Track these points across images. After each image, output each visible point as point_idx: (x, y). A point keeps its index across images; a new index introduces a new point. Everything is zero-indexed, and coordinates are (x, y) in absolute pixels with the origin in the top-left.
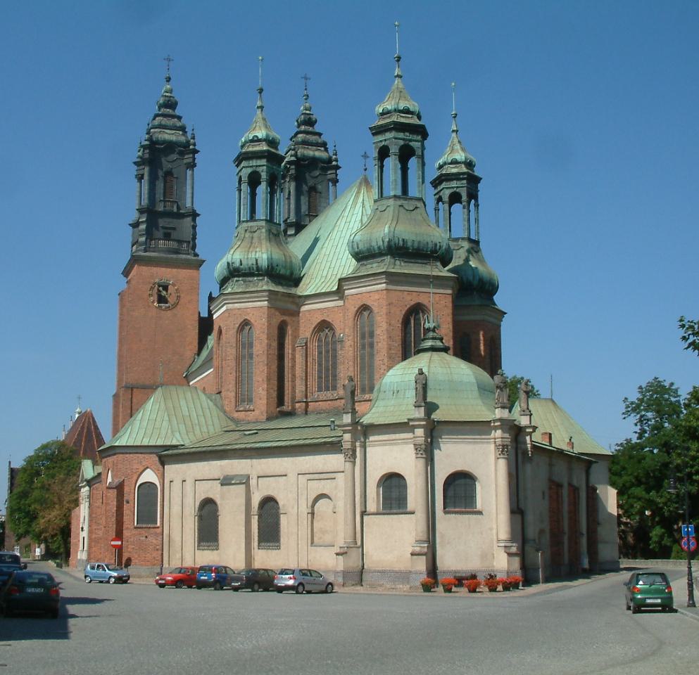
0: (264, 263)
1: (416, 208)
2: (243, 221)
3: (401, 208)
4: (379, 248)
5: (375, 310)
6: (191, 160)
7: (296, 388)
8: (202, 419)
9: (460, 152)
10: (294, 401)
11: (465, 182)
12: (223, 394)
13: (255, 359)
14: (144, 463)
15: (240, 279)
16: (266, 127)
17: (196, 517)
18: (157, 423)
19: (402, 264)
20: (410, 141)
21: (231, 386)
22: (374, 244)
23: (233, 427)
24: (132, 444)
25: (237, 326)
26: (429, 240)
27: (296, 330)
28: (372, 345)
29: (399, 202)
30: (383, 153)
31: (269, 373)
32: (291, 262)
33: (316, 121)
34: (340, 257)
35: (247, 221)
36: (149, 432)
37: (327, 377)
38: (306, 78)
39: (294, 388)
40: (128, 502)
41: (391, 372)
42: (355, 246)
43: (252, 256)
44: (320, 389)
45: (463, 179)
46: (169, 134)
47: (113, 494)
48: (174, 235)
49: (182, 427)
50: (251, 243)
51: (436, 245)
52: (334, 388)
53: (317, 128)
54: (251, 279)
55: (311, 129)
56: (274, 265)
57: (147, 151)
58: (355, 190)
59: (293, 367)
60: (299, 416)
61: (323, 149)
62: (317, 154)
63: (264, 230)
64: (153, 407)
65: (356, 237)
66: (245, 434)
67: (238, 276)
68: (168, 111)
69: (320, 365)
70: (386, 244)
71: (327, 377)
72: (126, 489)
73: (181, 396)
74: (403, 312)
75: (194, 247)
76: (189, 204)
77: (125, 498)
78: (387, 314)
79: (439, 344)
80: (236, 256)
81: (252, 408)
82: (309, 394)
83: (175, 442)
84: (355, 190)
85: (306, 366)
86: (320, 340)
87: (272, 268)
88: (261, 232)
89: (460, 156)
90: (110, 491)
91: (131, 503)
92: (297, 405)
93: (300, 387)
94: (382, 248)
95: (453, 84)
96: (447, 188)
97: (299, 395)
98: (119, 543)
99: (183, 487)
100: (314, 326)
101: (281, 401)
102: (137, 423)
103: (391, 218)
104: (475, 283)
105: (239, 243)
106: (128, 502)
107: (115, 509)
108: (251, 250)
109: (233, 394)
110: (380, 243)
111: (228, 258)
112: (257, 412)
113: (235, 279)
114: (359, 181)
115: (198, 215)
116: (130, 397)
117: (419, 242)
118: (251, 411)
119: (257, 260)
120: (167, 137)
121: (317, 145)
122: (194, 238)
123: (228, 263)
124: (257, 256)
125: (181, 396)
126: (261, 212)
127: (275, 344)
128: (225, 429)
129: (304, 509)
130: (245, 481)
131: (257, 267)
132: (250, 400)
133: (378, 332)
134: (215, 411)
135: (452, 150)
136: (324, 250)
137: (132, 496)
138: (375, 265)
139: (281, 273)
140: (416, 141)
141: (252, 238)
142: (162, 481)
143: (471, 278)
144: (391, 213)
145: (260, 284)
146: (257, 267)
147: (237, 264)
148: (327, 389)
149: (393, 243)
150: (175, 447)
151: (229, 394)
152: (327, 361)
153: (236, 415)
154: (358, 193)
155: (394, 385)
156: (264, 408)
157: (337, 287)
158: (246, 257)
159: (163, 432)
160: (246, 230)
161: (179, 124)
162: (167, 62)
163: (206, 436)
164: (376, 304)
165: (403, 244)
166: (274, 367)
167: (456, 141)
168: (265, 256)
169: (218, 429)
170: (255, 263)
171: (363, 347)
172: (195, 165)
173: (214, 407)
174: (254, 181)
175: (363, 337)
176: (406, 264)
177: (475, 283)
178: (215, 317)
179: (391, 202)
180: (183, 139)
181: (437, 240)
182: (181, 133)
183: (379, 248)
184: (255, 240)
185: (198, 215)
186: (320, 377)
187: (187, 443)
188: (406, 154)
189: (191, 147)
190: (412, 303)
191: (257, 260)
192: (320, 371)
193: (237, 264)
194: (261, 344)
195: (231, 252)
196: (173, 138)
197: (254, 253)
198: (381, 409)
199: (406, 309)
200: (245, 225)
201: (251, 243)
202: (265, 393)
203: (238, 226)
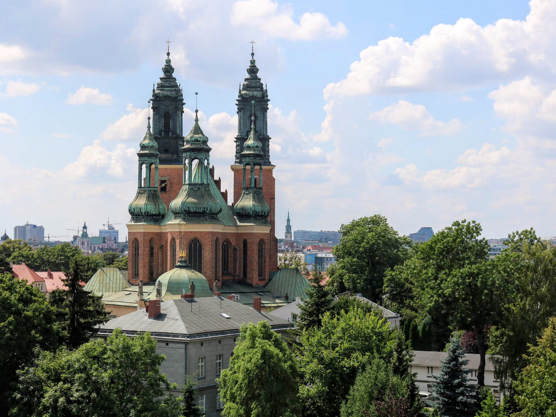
29: (191, 187)
38: (252, 43)
39: (158, 269)
56: (149, 211)
59: (158, 259)
62: (255, 93)
87: (148, 213)
121: (256, 87)
147: (133, 211)
149: (182, 209)
177: (251, 213)
181: (205, 206)
193: (133, 211)
196: (169, 93)
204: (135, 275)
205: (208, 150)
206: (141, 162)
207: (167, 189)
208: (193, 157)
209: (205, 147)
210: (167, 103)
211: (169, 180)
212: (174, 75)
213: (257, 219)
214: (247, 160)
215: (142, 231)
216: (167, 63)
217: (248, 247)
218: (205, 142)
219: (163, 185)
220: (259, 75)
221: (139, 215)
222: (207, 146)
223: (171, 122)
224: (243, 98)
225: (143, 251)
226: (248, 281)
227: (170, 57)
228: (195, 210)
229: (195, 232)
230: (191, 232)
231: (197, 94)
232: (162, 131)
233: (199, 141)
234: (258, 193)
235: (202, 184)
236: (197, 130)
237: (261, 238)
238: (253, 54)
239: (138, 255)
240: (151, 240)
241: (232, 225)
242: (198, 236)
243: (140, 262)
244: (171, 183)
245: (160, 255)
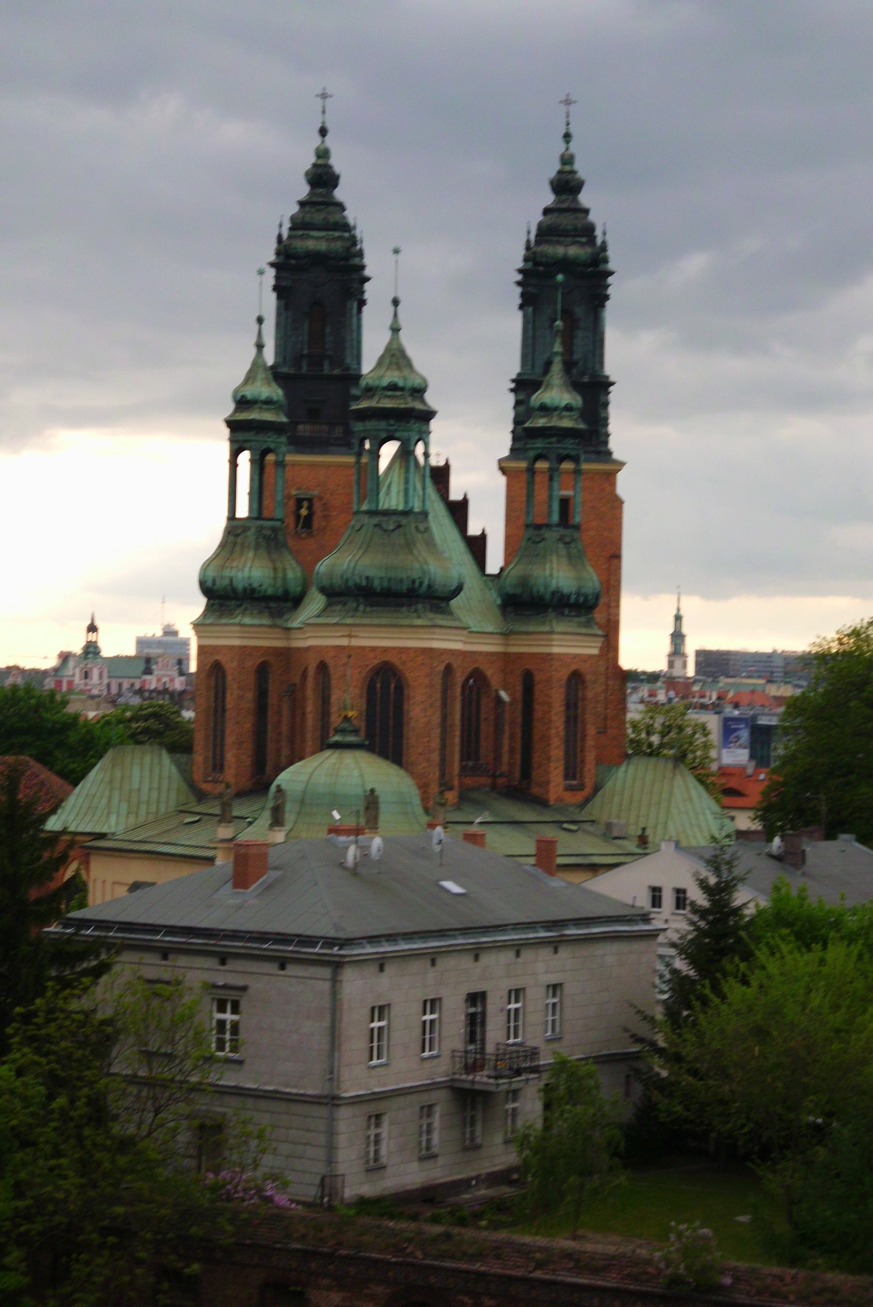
1: (399, 526)
8: (155, 794)
11: (553, 440)
13: (228, 714)
18: (96, 800)
19: (368, 609)
20: (396, 431)
26: (404, 576)
29: (376, 520)
32: (284, 578)
38: (568, 102)
39: (278, 750)
43: (227, 573)
45: (550, 436)
46: (318, 238)
51: (414, 581)
54: (228, 603)
56: (256, 585)
61: (584, 240)
62: (573, 251)
74: (364, 674)
83: (105, 830)
104: (548, 596)
117: (390, 579)
120: (311, 245)
128: (182, 808)
139: (270, 591)
140: (405, 431)
141: (235, 544)
143: (542, 590)
147: (209, 584)
150: (102, 836)
162: (319, 101)
165: (368, 583)
177: (548, 596)
181: (415, 575)
184: (238, 549)
190: (376, 662)
196: (322, 246)
204: (214, 768)
205: (428, 415)
206: (236, 446)
207: (316, 523)
208: (383, 435)
209: (418, 406)
210: (318, 275)
211: (320, 498)
212: (339, 194)
213: (562, 614)
214: (539, 443)
215: (237, 642)
216: (319, 156)
217: (537, 693)
218: (419, 392)
219: (304, 512)
220: (585, 198)
222: (423, 402)
223: (328, 330)
224: (537, 264)
225: (239, 697)
226: (536, 790)
227: (329, 141)
228: (385, 584)
229: (386, 650)
230: (373, 649)
231: (396, 251)
232: (302, 356)
233: (402, 389)
234: (568, 539)
235: (406, 513)
236: (395, 356)
237: (574, 667)
238: (567, 136)
239: (224, 710)
240: (262, 670)
241: (490, 629)
242: (395, 660)
243: (228, 731)
244: (326, 508)
245: (286, 712)
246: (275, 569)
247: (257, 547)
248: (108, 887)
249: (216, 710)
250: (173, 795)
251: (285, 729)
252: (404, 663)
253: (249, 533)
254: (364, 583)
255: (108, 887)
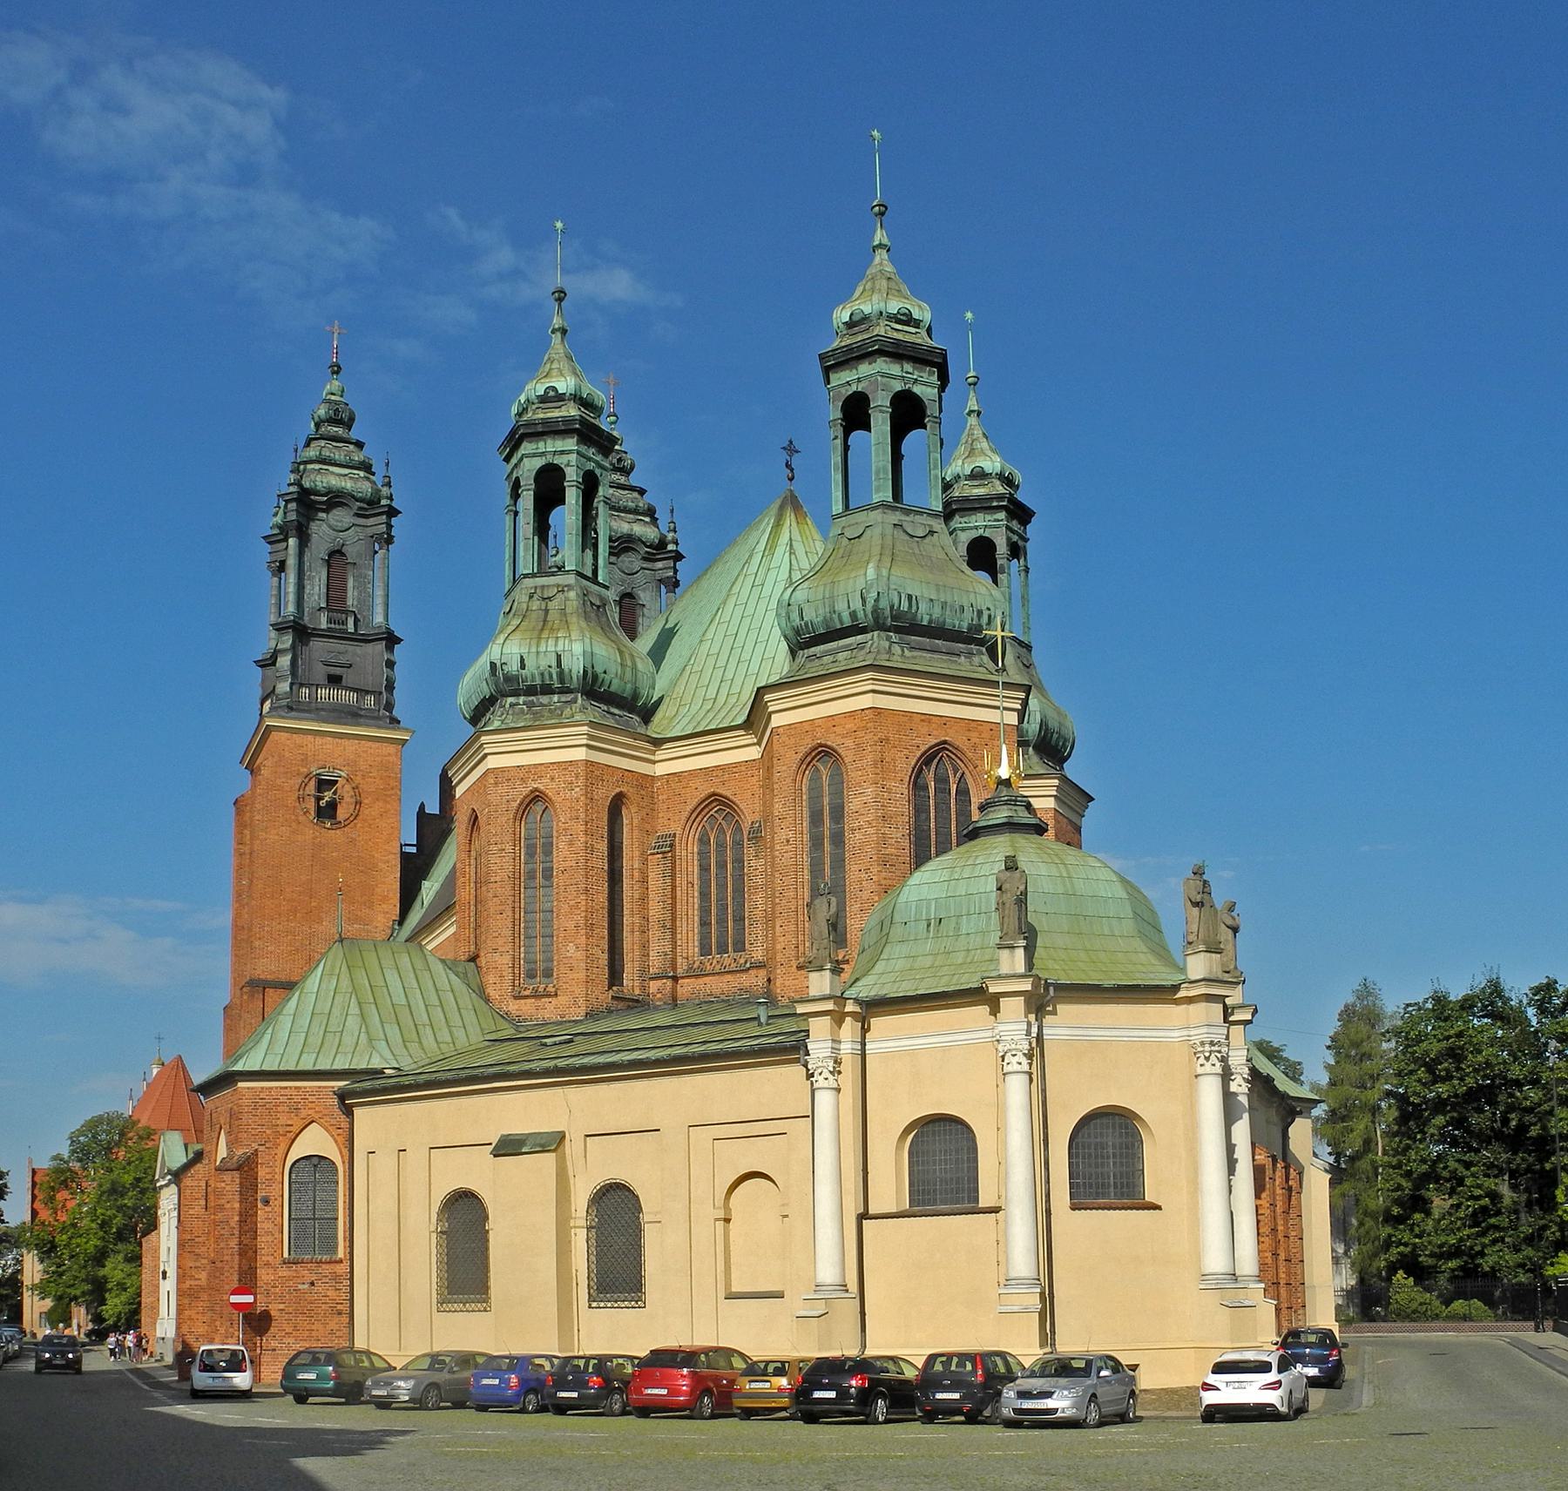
0: (575, 665)
1: (932, 533)
2: (526, 576)
3: (899, 533)
4: (853, 615)
5: (848, 757)
6: (383, 528)
7: (646, 950)
8: (438, 1014)
9: (989, 453)
10: (645, 976)
12: (482, 961)
14: (304, 1113)
15: (521, 699)
16: (575, 374)
17: (434, 1235)
21: (500, 941)
22: (841, 606)
23: (509, 1032)
24: (275, 1068)
25: (515, 805)
27: (650, 814)
28: (838, 839)
30: (856, 413)
31: (590, 912)
33: (632, 468)
34: (746, 656)
35: (533, 575)
36: (315, 1040)
37: (722, 921)
39: (645, 946)
40: (266, 1202)
41: (917, 877)
42: (795, 616)
44: (705, 950)
47: (230, 1184)
48: (349, 678)
49: (393, 1032)
50: (545, 621)
51: (980, 613)
52: (740, 946)
53: (634, 480)
54: (544, 699)
55: (623, 480)
56: (599, 670)
57: (293, 506)
58: (768, 522)
59: (644, 899)
60: (656, 1008)
63: (572, 594)
64: (324, 986)
65: (797, 593)
66: (545, 1045)
67: (516, 693)
68: (338, 430)
69: (705, 895)
70: (870, 603)
71: (722, 921)
72: (262, 1173)
73: (387, 962)
75: (389, 706)
76: (379, 619)
77: (260, 1195)
78: (875, 764)
79: (1023, 817)
80: (509, 649)
81: (551, 989)
82: (679, 960)
83: (376, 1063)
84: (768, 522)
85: (674, 898)
86: (704, 841)
87: (595, 677)
88: (567, 599)
89: (992, 463)
90: (227, 1177)
91: (274, 1203)
92: (654, 986)
93: (658, 947)
94: (861, 614)
95: (969, 315)
96: (963, 530)
97: (656, 963)
98: (249, 1299)
99: (403, 1164)
100: (689, 808)
101: (615, 976)
102: (285, 1021)
103: (876, 550)
105: (516, 622)
106: (266, 1202)
107: (237, 1218)
108: (545, 635)
109: (507, 959)
110: (857, 604)
111: (494, 652)
112: (562, 999)
113: (510, 700)
114: (778, 502)
115: (399, 641)
116: (261, 992)
117: (944, 605)
118: (549, 996)
119: (559, 657)
122: (390, 687)
123: (493, 665)
124: (560, 648)
125: (387, 962)
126: (568, 550)
127: (603, 847)
129: (707, 1213)
130: (553, 1143)
131: (561, 674)
132: (548, 973)
133: (853, 804)
134: (467, 998)
135: (972, 452)
136: (705, 646)
137: (277, 1186)
138: (841, 656)
139: (612, 689)
141: (547, 611)
142: (346, 1152)
144: (877, 541)
145: (567, 712)
146: (561, 674)
147: (514, 667)
148: (723, 949)
149: (884, 604)
150: (377, 1073)
151: (499, 961)
152: (722, 887)
153: (513, 1007)
154: (778, 524)
155: (928, 908)
156: (579, 990)
157: (744, 717)
158: (534, 650)
159: (348, 1040)
160: (531, 597)
161: (358, 457)
163: (448, 1050)
164: (849, 743)
166: (603, 898)
167: (978, 433)
168: (577, 648)
169: (476, 1038)
170: (554, 664)
171: (816, 842)
172: (389, 540)
173: (464, 988)
174: (549, 488)
175: (816, 818)
176: (915, 653)
178: (459, 791)
179: (876, 516)
180: (365, 488)
181: (982, 603)
182: (362, 474)
183: (853, 615)
185: (399, 641)
186: (705, 923)
187: (407, 1064)
188: (908, 414)
189: (384, 502)
191: (559, 657)
192: (705, 911)
194: (571, 843)
195: (501, 640)
197: (551, 642)
198: (900, 964)
199: (919, 754)
200: (528, 582)
201: (545, 621)
202: (580, 955)
203: (510, 591)
204: (531, 975)
207: (342, 813)
215: (580, 754)
219: (328, 796)
221: (547, 690)
229: (945, 721)
230: (927, 718)
239: (548, 874)
246: (621, 652)
247: (587, 618)
248: (416, 1157)
249: (531, 875)
250: (470, 1017)
251: (655, 909)
252: (975, 746)
253: (572, 594)
254: (905, 606)
255: (416, 1159)
